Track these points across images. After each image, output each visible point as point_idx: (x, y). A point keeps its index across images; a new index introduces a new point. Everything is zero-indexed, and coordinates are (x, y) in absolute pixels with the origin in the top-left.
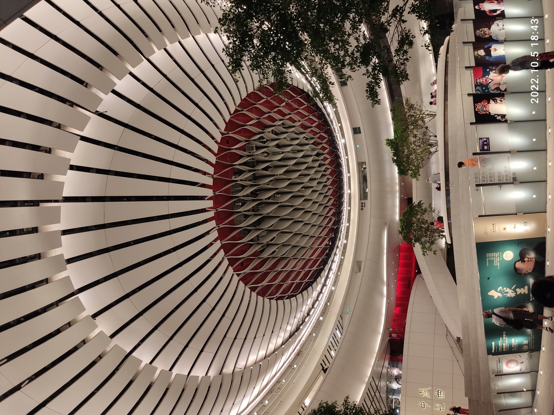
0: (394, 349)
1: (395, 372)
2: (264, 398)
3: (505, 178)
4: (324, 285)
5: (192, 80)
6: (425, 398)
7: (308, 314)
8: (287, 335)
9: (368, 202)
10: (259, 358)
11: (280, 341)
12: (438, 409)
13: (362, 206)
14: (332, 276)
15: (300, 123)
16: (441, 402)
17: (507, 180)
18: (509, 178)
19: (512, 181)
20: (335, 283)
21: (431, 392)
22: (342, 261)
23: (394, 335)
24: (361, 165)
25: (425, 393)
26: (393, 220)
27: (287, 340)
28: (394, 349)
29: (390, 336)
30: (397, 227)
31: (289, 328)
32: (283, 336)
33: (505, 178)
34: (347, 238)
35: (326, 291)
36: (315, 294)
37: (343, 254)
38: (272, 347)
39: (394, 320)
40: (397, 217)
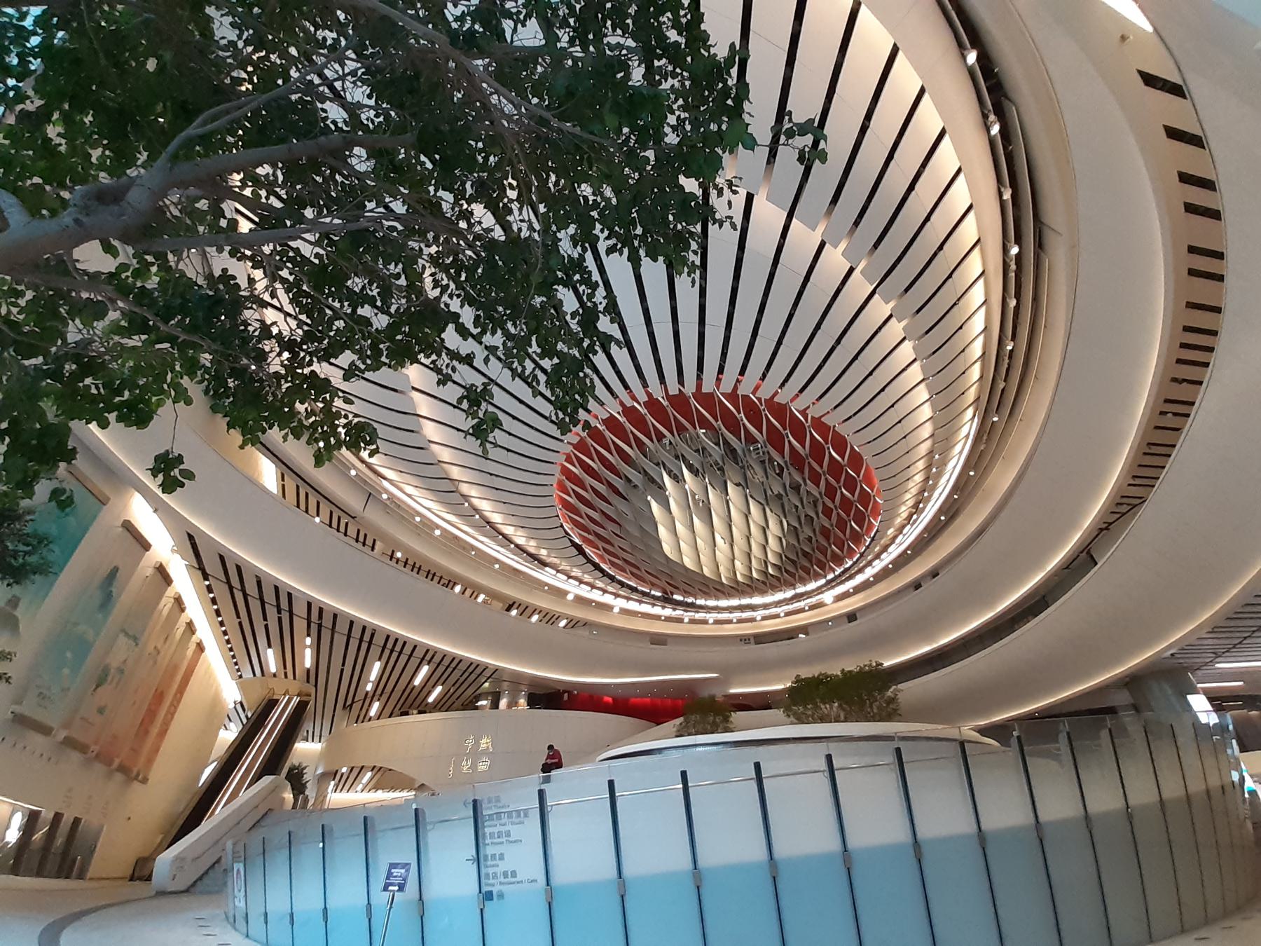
0: (547, 697)
1: (522, 701)
2: (444, 530)
3: (491, 871)
4: (617, 595)
5: (818, 327)
6: (477, 744)
7: (570, 577)
8: (532, 550)
9: (753, 646)
10: (487, 514)
11: (521, 541)
12: (464, 763)
13: (745, 639)
14: (633, 606)
15: (827, 525)
16: (474, 766)
17: (487, 875)
18: (491, 881)
19: (485, 889)
20: (624, 612)
21: (485, 752)
22: (658, 618)
23: (566, 696)
24: (804, 629)
25: (485, 743)
26: (730, 685)
27: (524, 551)
28: (547, 697)
29: (565, 691)
30: (718, 693)
31: (544, 552)
32: (531, 546)
33: (491, 871)
34: (692, 621)
35: (608, 599)
36: (587, 578)
37: (669, 619)
38: (509, 530)
39: (591, 697)
40: (733, 691)
